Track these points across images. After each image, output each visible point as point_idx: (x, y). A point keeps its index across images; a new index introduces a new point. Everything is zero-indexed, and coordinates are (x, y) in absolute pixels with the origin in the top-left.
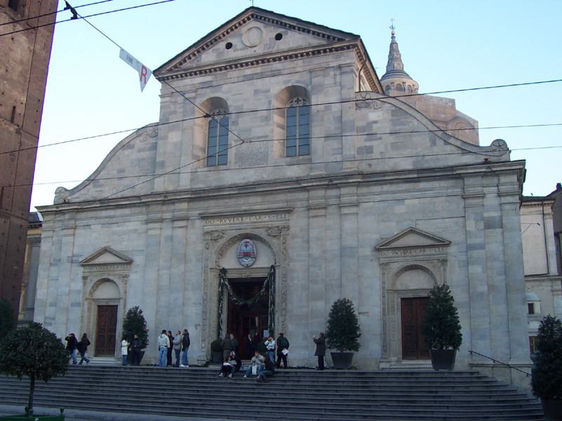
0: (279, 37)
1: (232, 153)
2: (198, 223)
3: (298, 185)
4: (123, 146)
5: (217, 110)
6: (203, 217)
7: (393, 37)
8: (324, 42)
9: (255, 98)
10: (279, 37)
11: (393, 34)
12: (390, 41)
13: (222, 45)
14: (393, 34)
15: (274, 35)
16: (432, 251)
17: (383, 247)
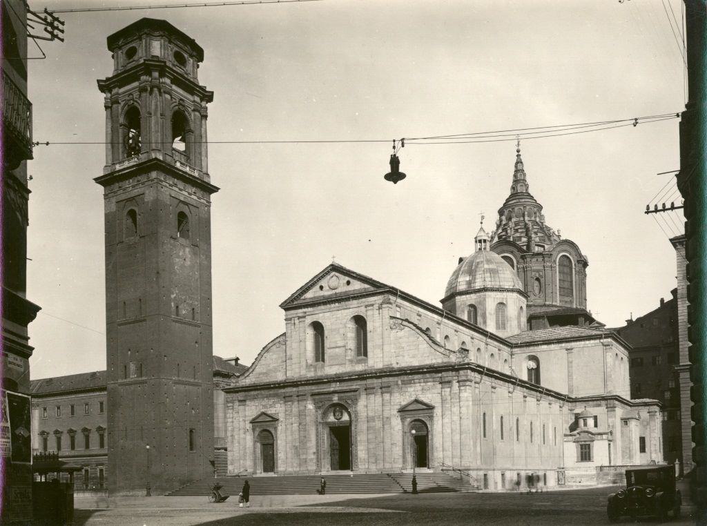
0: (348, 283)
1: (326, 357)
2: (310, 398)
3: (362, 377)
4: (266, 349)
5: (318, 327)
6: (312, 395)
7: (519, 156)
8: (372, 289)
9: (338, 321)
10: (348, 283)
11: (518, 151)
12: (515, 159)
13: (317, 287)
14: (518, 151)
15: (345, 282)
16: (426, 411)
17: (403, 410)
